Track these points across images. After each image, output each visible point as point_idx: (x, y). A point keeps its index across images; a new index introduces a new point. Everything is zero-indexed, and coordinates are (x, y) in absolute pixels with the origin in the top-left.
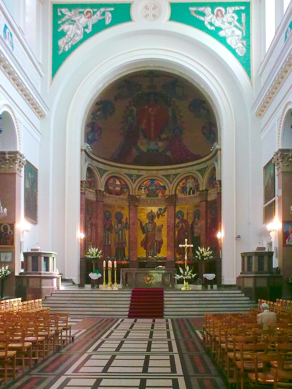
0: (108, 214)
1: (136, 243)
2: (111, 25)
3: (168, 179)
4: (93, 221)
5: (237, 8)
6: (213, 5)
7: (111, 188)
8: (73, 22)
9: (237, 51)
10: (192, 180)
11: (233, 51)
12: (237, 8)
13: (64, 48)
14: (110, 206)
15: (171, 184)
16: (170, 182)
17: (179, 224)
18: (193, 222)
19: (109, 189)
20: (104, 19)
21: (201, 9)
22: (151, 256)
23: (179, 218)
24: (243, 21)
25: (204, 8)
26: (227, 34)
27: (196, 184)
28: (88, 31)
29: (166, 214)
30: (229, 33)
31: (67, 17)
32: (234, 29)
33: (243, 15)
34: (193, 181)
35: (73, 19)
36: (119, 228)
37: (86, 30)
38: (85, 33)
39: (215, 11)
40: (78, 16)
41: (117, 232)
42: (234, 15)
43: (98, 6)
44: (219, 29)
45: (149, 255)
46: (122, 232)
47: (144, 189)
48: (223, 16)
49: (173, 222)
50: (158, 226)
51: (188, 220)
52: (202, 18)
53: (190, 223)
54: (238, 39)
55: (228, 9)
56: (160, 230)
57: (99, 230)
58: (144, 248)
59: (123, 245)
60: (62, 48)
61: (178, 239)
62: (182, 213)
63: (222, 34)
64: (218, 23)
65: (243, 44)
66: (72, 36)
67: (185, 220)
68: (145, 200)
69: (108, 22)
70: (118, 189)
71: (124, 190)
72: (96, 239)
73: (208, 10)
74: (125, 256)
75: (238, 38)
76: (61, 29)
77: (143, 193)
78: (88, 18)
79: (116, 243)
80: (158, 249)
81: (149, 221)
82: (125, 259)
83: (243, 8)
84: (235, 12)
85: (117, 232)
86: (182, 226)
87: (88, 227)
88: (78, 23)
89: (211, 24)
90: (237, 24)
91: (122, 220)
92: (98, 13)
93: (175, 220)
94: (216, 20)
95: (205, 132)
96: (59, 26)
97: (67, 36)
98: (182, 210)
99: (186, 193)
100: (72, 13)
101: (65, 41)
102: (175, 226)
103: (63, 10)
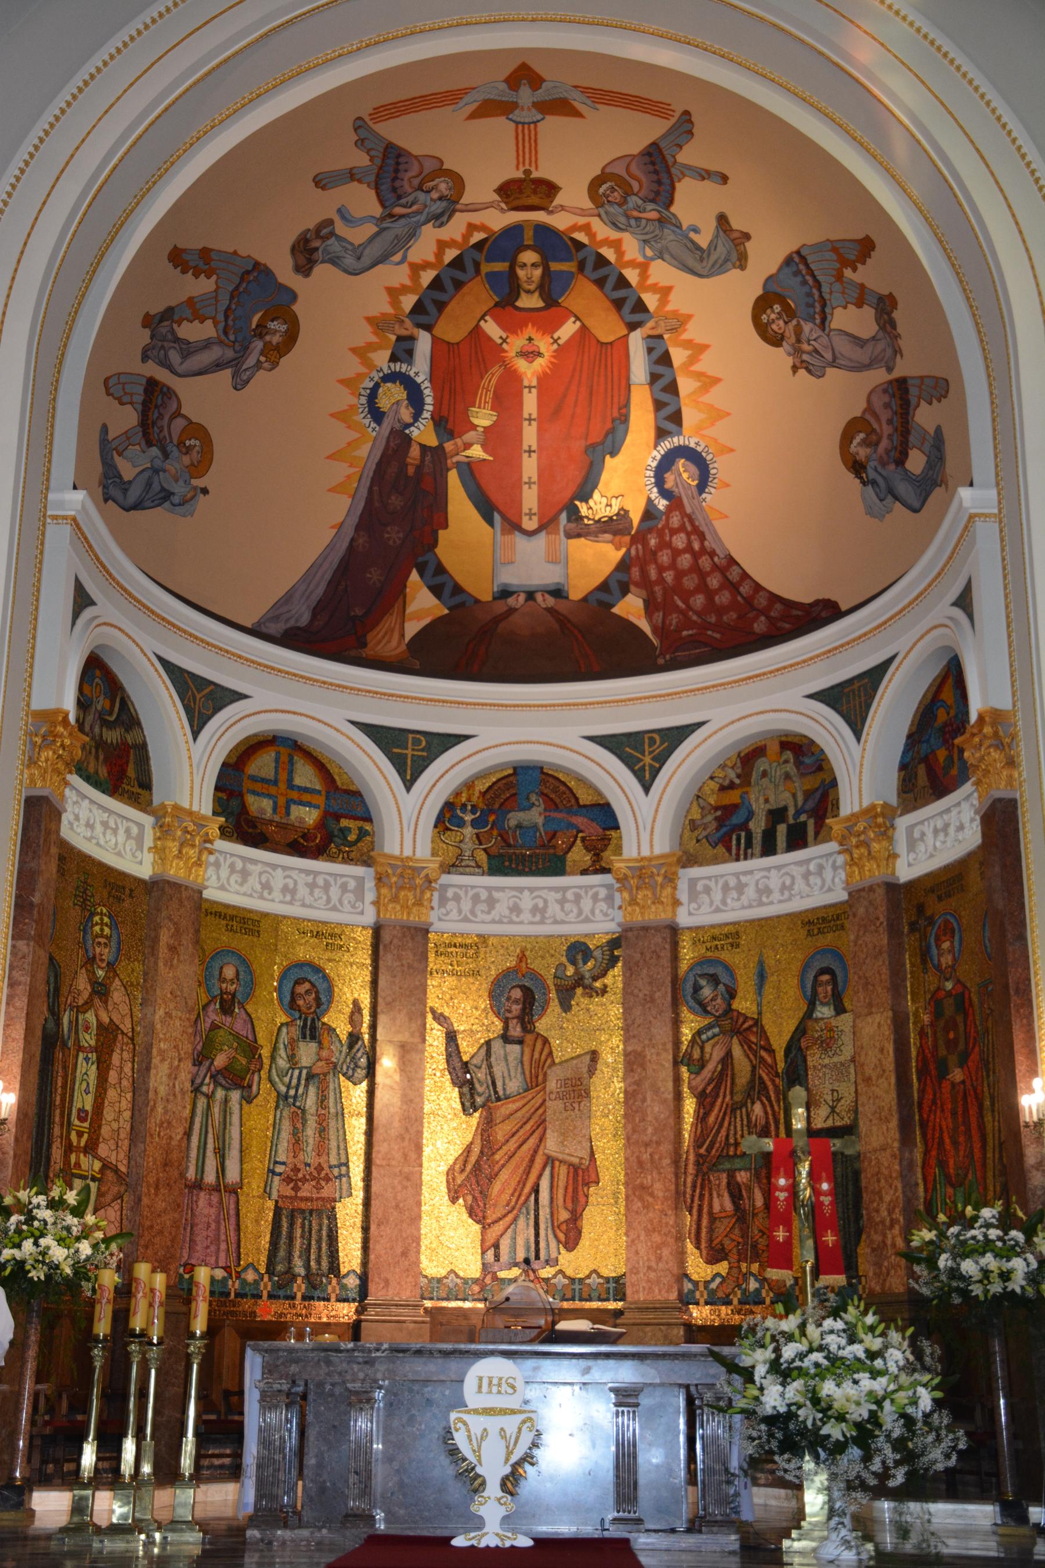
0: (229, 972)
3: (629, 762)
7: (260, 806)
10: (786, 762)
15: (647, 789)
16: (639, 775)
17: (702, 1048)
18: (800, 1031)
19: (247, 813)
22: (516, 1265)
23: (703, 1008)
27: (812, 782)
29: (615, 978)
34: (790, 767)
36: (301, 1069)
41: (292, 1092)
45: (504, 1257)
46: (322, 1101)
47: (474, 823)
50: (561, 1063)
51: (767, 1021)
53: (779, 1042)
57: (159, 1080)
58: (471, 1213)
59: (325, 1193)
61: (698, 1142)
62: (720, 971)
67: (746, 1018)
68: (484, 895)
71: (344, 823)
72: (136, 1135)
74: (334, 1267)
77: (468, 846)
79: (279, 1169)
80: (564, 1215)
81: (506, 1028)
82: (332, 1287)
85: (292, 1092)
86: (728, 1057)
87: (80, 1049)
91: (325, 1020)
93: (676, 1023)
98: (725, 956)
99: (749, 844)
102: (676, 1063)
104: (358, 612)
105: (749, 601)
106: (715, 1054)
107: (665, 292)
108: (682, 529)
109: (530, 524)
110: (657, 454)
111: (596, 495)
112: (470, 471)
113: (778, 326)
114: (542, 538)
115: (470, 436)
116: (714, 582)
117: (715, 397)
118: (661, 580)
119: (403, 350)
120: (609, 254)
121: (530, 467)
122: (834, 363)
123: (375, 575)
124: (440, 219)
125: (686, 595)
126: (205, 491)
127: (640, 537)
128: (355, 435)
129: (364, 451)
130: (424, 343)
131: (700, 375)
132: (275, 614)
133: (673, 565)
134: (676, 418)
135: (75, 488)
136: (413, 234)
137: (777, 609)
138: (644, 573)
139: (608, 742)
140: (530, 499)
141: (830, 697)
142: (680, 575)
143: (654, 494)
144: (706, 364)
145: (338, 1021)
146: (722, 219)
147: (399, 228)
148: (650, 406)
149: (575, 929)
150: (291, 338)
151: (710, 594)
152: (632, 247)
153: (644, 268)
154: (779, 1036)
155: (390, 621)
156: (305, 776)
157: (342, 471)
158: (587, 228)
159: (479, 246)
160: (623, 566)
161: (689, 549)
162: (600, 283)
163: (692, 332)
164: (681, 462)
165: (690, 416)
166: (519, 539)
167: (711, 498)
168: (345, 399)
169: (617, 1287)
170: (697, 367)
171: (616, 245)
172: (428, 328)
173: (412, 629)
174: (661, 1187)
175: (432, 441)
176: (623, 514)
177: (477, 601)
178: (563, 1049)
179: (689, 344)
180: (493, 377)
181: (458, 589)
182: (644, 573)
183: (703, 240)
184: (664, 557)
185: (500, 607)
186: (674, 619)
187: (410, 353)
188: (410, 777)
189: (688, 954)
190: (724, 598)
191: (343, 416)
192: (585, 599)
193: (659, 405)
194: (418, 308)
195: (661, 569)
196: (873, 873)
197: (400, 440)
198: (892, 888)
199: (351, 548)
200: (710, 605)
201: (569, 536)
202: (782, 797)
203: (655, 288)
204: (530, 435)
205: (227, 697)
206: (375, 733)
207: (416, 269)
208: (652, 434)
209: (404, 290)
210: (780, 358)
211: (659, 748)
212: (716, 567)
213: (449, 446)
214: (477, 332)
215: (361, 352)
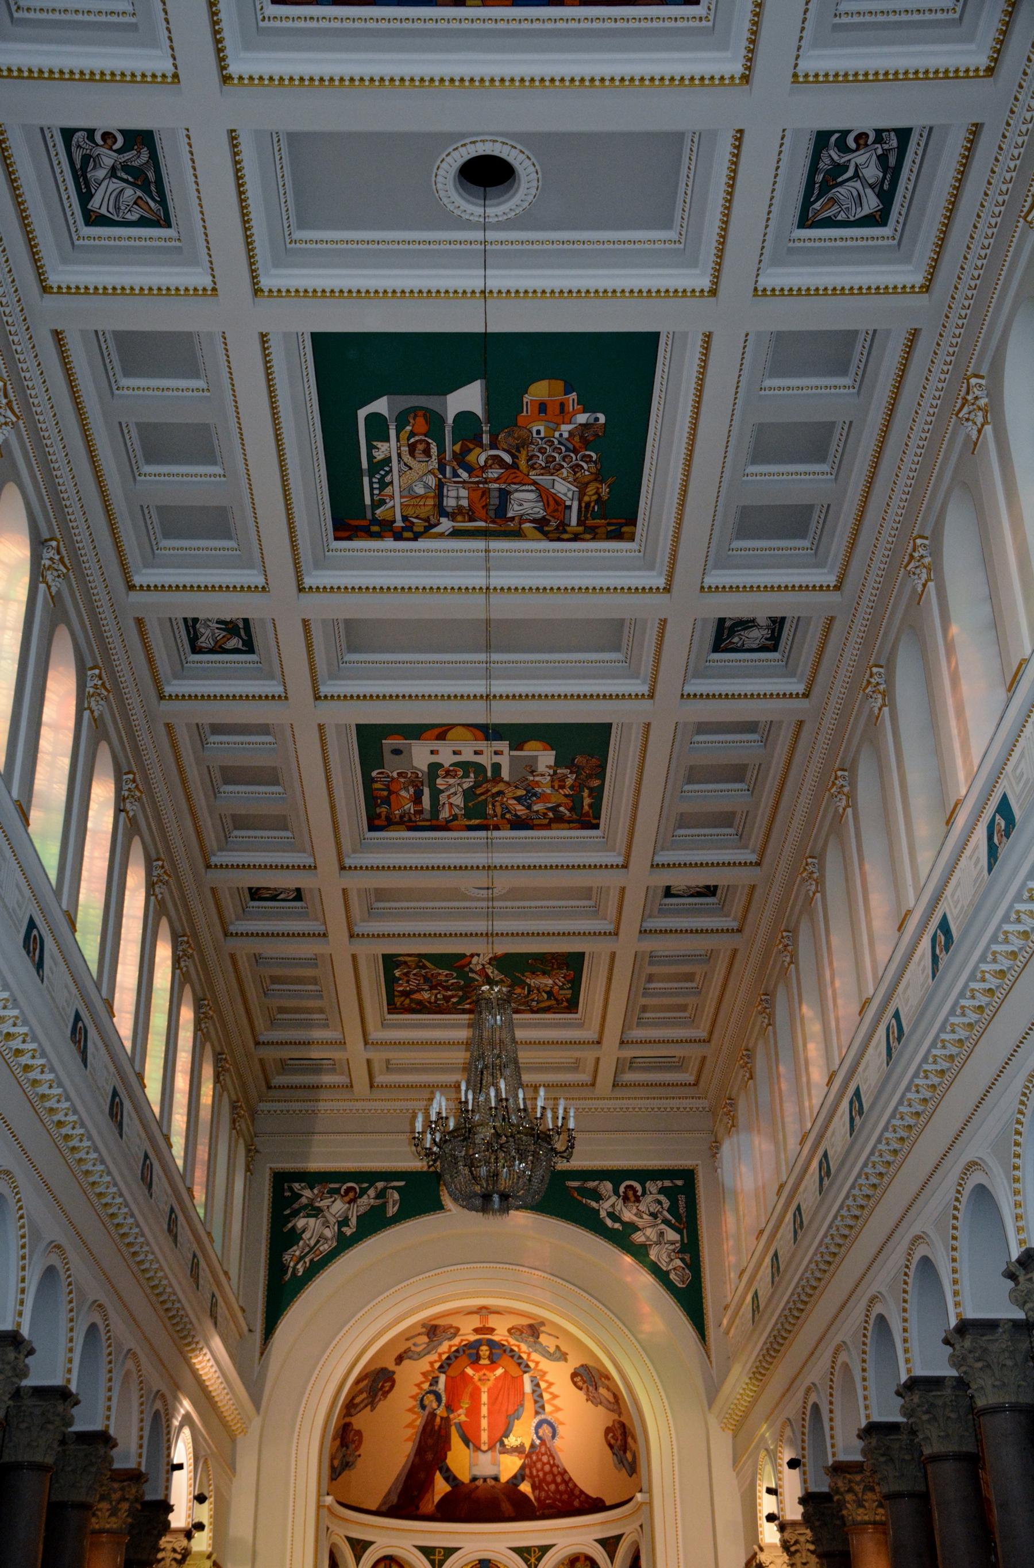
5: (667, 1183)
6: (616, 1176)
8: (316, 1212)
9: (672, 1276)
12: (667, 1183)
13: (294, 1268)
20: (384, 1206)
21: (591, 1184)
24: (682, 1210)
25: (596, 1183)
26: (648, 1238)
28: (348, 1231)
30: (654, 1237)
31: (304, 1200)
32: (663, 1226)
33: (682, 1199)
35: (317, 1204)
37: (344, 1229)
38: (340, 1236)
39: (622, 1189)
40: (326, 1198)
42: (662, 1198)
43: (370, 1177)
44: (633, 1228)
48: (637, 1200)
52: (594, 1204)
54: (674, 1251)
55: (648, 1184)
60: (290, 1270)
63: (638, 1238)
64: (628, 1216)
65: (682, 1260)
66: (312, 1242)
69: (392, 1210)
73: (606, 1187)
75: (672, 1247)
76: (290, 1225)
78: (349, 1203)
83: (680, 1183)
84: (662, 1191)
88: (326, 1213)
89: (612, 1215)
90: (670, 1217)
92: (372, 1192)
94: (624, 1209)
95: (612, 1442)
97: (301, 1243)
100: (316, 1191)
101: (297, 1253)
103: (296, 1186)
104: (416, 1493)
105: (572, 1491)
107: (537, 1363)
108: (546, 1454)
109: (484, 1447)
110: (536, 1421)
111: (511, 1436)
112: (460, 1426)
113: (580, 1384)
114: (489, 1454)
115: (461, 1411)
116: (559, 1479)
117: (556, 1402)
118: (538, 1476)
119: (435, 1381)
120: (516, 1349)
121: (484, 1423)
122: (601, 1403)
124: (450, 1339)
125: (548, 1484)
126: (359, 1456)
127: (529, 1456)
128: (415, 1416)
129: (418, 1422)
130: (442, 1378)
131: (551, 1393)
132: (384, 1503)
133: (542, 1469)
134: (543, 1407)
135: (328, 1494)
136: (440, 1344)
137: (583, 1498)
138: (531, 1472)
139: (515, 1550)
140: (484, 1436)
141: (603, 1542)
142: (545, 1474)
143: (535, 1437)
144: (553, 1389)
146: (557, 1347)
147: (435, 1343)
148: (532, 1402)
150: (392, 1387)
151: (557, 1485)
152: (524, 1347)
153: (529, 1354)
155: (428, 1496)
157: (410, 1431)
158: (507, 1341)
159: (465, 1345)
160: (523, 1467)
161: (548, 1463)
162: (512, 1357)
163: (547, 1377)
164: (545, 1426)
165: (548, 1408)
166: (480, 1454)
167: (557, 1442)
168: (412, 1403)
170: (550, 1390)
171: (519, 1346)
172: (444, 1373)
173: (437, 1498)
175: (445, 1415)
176: (522, 1445)
177: (463, 1483)
179: (546, 1381)
180: (469, 1389)
181: (455, 1478)
182: (531, 1472)
183: (552, 1350)
184: (539, 1465)
185: (473, 1485)
186: (543, 1494)
187: (437, 1382)
190: (562, 1488)
191: (410, 1410)
192: (507, 1482)
193: (536, 1402)
194: (441, 1367)
195: (538, 1471)
197: (433, 1415)
199: (413, 1465)
200: (557, 1490)
201: (501, 1453)
203: (533, 1361)
204: (484, 1410)
207: (440, 1355)
208: (533, 1412)
209: (436, 1361)
210: (581, 1395)
211: (538, 1554)
212: (559, 1473)
213: (451, 1416)
214: (463, 1373)
215: (418, 1385)
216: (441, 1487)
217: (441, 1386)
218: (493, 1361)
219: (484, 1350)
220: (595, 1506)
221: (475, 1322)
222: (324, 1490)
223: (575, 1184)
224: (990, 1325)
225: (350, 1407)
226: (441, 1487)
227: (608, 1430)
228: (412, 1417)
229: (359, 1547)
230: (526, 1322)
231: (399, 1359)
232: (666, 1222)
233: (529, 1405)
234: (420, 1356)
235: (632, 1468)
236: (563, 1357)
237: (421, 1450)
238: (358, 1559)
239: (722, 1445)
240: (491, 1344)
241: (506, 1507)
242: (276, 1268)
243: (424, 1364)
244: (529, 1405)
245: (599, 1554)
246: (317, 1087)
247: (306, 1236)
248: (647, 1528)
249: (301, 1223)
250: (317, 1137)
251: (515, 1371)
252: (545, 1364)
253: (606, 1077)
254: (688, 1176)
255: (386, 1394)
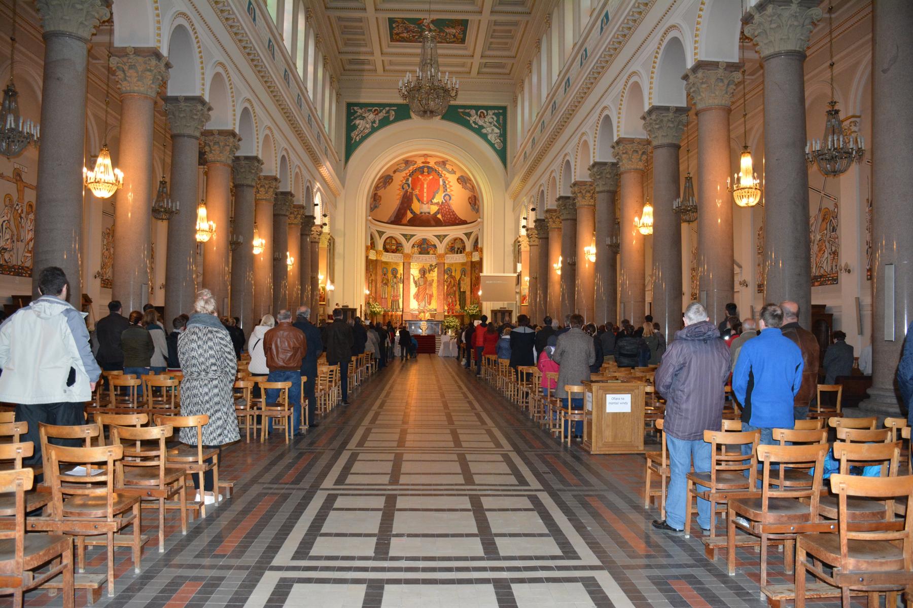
1: (409, 296)
2: (394, 121)
4: (373, 277)
5: (496, 111)
6: (477, 108)
7: (388, 247)
8: (363, 118)
9: (496, 145)
11: (492, 145)
12: (496, 111)
14: (386, 263)
20: (389, 117)
21: (467, 111)
28: (375, 126)
29: (436, 270)
30: (490, 131)
31: (358, 114)
33: (501, 117)
38: (372, 126)
43: (383, 106)
44: (482, 127)
48: (485, 117)
49: (442, 278)
56: (431, 285)
63: (484, 131)
64: (481, 123)
69: (392, 118)
70: (394, 247)
73: (473, 112)
83: (501, 111)
84: (494, 114)
89: (475, 122)
92: (384, 111)
96: (352, 120)
103: (355, 108)
106: (449, 280)
110: (443, 195)
112: (416, 195)
119: (407, 180)
121: (425, 195)
123: (403, 211)
127: (441, 206)
130: (410, 179)
132: (389, 219)
140: (425, 199)
141: (466, 234)
144: (451, 184)
145: (399, 276)
149: (431, 263)
152: (440, 169)
154: (458, 278)
156: (394, 242)
157: (398, 197)
163: (449, 179)
165: (448, 190)
169: (436, 310)
173: (408, 219)
174: (442, 297)
178: (429, 279)
180: (420, 183)
188: (408, 240)
189: (446, 267)
191: (399, 189)
196: (469, 260)
197: (407, 191)
198: (472, 262)
202: (459, 246)
204: (425, 190)
205: (383, 233)
206: (403, 235)
210: (460, 186)
216: (409, 215)
217: (410, 181)
218: (429, 174)
219: (426, 169)
220: (464, 222)
221: (423, 160)
222: (368, 214)
223: (462, 110)
224: (605, 164)
225: (377, 188)
226: (409, 215)
227: (469, 198)
228: (399, 192)
229: (381, 233)
230: (442, 160)
231: (395, 172)
232: (495, 125)
233: (441, 189)
234: (402, 171)
235: (477, 211)
236: (455, 173)
237: (402, 203)
238: (380, 237)
239: (509, 204)
240: (428, 167)
241: (433, 222)
242: (349, 138)
243: (404, 174)
244: (441, 189)
245: (465, 238)
246: (363, 70)
247: (360, 127)
248: (481, 230)
249: (357, 122)
250: (363, 90)
251: (436, 177)
252: (448, 175)
253: (475, 70)
254: (504, 109)
255: (389, 184)
